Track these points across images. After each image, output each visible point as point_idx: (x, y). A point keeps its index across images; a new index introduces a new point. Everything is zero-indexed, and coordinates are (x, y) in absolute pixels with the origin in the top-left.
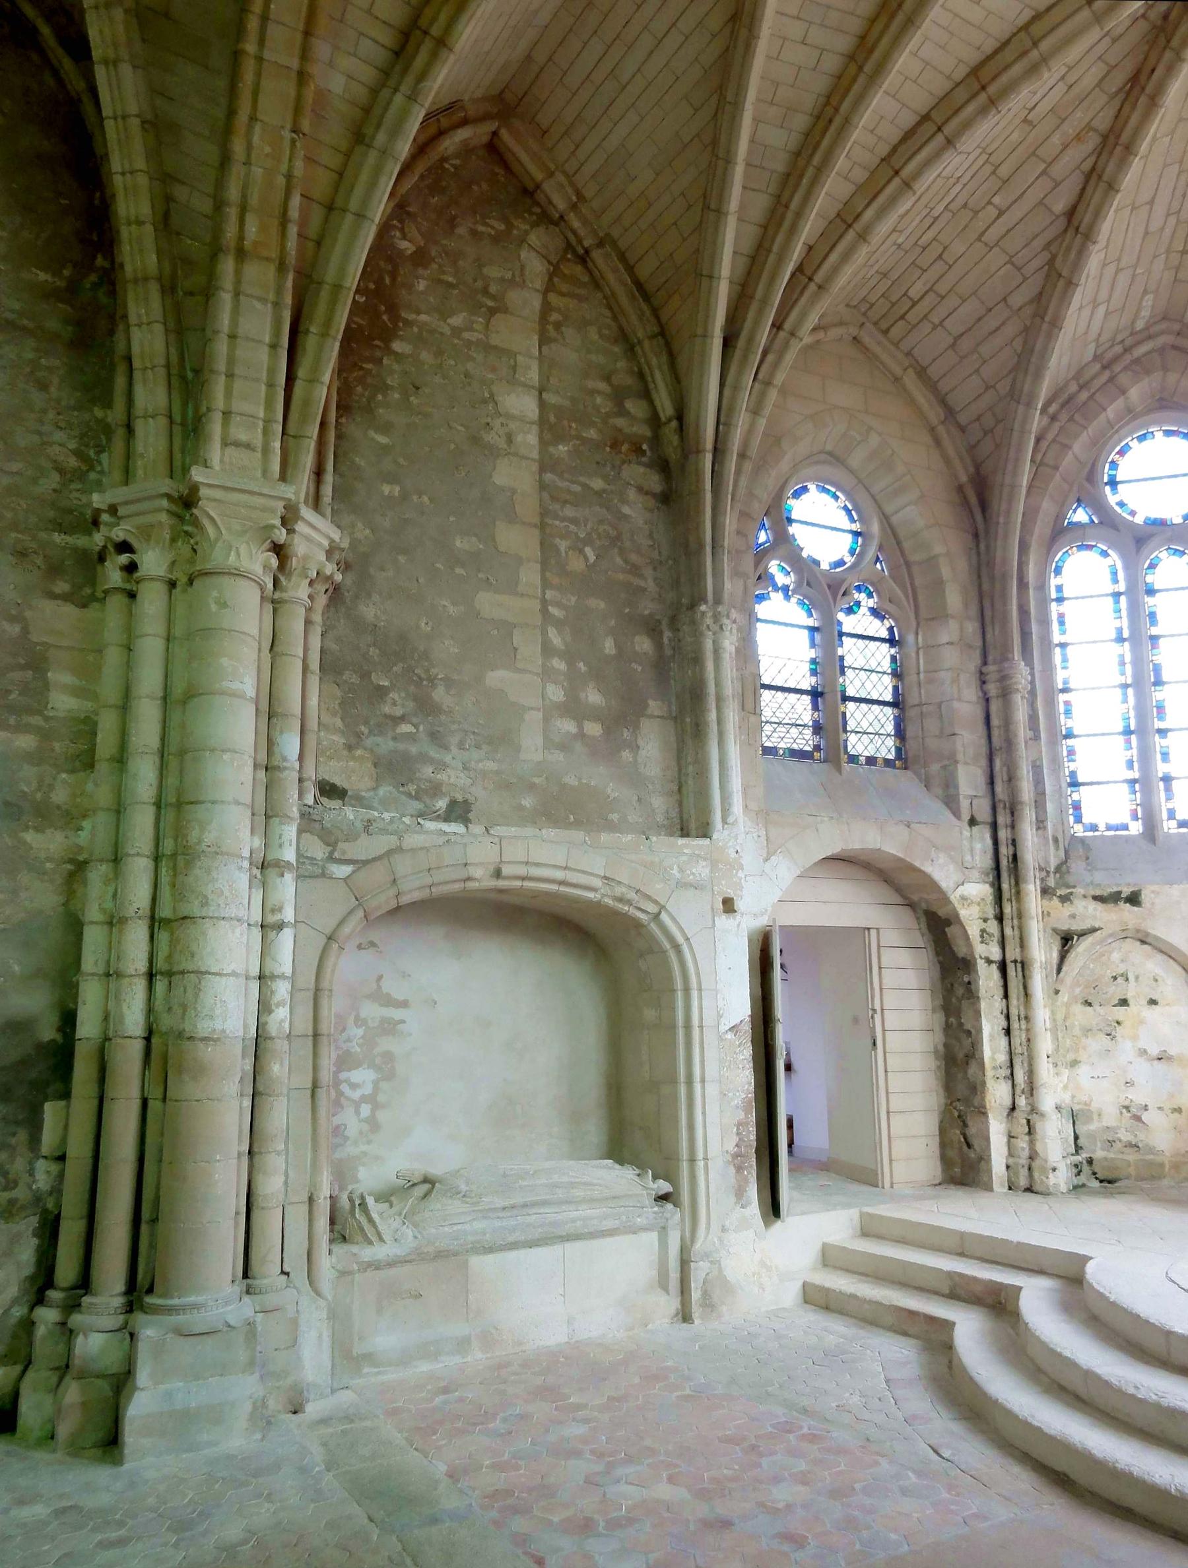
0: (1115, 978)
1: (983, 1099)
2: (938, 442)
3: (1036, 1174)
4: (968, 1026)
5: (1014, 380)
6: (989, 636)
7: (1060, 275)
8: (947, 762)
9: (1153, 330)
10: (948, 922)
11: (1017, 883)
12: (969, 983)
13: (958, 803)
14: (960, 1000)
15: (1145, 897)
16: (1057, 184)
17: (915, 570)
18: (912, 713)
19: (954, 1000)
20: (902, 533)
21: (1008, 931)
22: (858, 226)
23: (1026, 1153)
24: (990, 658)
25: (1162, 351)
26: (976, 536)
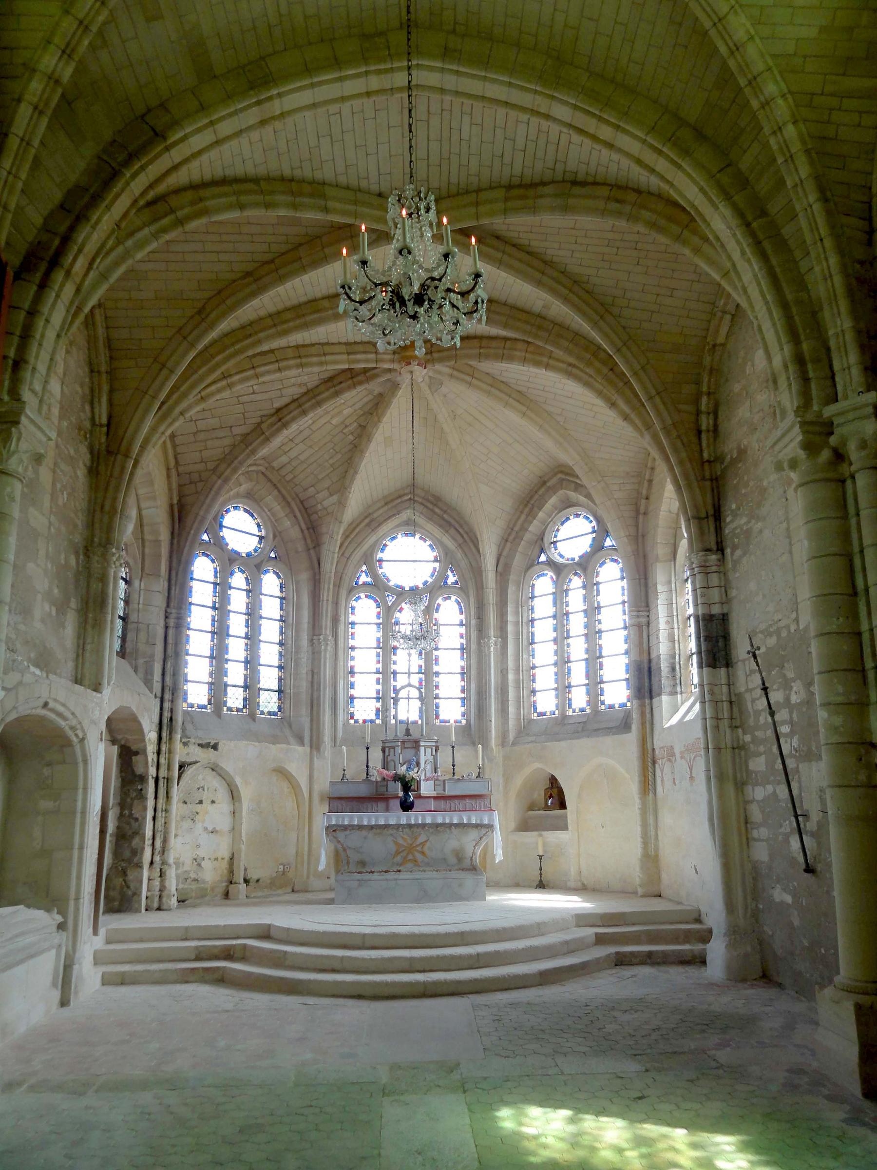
1: (141, 858)
2: (169, 476)
3: (164, 899)
4: (137, 815)
5: (219, 465)
6: (173, 592)
7: (263, 433)
10: (136, 753)
11: (170, 733)
13: (152, 684)
15: (220, 747)
16: (282, 396)
17: (147, 544)
18: (131, 626)
19: (129, 800)
20: (145, 521)
21: (162, 760)
22: (229, 380)
23: (158, 888)
24: (172, 605)
25: (257, 472)
26: (172, 533)
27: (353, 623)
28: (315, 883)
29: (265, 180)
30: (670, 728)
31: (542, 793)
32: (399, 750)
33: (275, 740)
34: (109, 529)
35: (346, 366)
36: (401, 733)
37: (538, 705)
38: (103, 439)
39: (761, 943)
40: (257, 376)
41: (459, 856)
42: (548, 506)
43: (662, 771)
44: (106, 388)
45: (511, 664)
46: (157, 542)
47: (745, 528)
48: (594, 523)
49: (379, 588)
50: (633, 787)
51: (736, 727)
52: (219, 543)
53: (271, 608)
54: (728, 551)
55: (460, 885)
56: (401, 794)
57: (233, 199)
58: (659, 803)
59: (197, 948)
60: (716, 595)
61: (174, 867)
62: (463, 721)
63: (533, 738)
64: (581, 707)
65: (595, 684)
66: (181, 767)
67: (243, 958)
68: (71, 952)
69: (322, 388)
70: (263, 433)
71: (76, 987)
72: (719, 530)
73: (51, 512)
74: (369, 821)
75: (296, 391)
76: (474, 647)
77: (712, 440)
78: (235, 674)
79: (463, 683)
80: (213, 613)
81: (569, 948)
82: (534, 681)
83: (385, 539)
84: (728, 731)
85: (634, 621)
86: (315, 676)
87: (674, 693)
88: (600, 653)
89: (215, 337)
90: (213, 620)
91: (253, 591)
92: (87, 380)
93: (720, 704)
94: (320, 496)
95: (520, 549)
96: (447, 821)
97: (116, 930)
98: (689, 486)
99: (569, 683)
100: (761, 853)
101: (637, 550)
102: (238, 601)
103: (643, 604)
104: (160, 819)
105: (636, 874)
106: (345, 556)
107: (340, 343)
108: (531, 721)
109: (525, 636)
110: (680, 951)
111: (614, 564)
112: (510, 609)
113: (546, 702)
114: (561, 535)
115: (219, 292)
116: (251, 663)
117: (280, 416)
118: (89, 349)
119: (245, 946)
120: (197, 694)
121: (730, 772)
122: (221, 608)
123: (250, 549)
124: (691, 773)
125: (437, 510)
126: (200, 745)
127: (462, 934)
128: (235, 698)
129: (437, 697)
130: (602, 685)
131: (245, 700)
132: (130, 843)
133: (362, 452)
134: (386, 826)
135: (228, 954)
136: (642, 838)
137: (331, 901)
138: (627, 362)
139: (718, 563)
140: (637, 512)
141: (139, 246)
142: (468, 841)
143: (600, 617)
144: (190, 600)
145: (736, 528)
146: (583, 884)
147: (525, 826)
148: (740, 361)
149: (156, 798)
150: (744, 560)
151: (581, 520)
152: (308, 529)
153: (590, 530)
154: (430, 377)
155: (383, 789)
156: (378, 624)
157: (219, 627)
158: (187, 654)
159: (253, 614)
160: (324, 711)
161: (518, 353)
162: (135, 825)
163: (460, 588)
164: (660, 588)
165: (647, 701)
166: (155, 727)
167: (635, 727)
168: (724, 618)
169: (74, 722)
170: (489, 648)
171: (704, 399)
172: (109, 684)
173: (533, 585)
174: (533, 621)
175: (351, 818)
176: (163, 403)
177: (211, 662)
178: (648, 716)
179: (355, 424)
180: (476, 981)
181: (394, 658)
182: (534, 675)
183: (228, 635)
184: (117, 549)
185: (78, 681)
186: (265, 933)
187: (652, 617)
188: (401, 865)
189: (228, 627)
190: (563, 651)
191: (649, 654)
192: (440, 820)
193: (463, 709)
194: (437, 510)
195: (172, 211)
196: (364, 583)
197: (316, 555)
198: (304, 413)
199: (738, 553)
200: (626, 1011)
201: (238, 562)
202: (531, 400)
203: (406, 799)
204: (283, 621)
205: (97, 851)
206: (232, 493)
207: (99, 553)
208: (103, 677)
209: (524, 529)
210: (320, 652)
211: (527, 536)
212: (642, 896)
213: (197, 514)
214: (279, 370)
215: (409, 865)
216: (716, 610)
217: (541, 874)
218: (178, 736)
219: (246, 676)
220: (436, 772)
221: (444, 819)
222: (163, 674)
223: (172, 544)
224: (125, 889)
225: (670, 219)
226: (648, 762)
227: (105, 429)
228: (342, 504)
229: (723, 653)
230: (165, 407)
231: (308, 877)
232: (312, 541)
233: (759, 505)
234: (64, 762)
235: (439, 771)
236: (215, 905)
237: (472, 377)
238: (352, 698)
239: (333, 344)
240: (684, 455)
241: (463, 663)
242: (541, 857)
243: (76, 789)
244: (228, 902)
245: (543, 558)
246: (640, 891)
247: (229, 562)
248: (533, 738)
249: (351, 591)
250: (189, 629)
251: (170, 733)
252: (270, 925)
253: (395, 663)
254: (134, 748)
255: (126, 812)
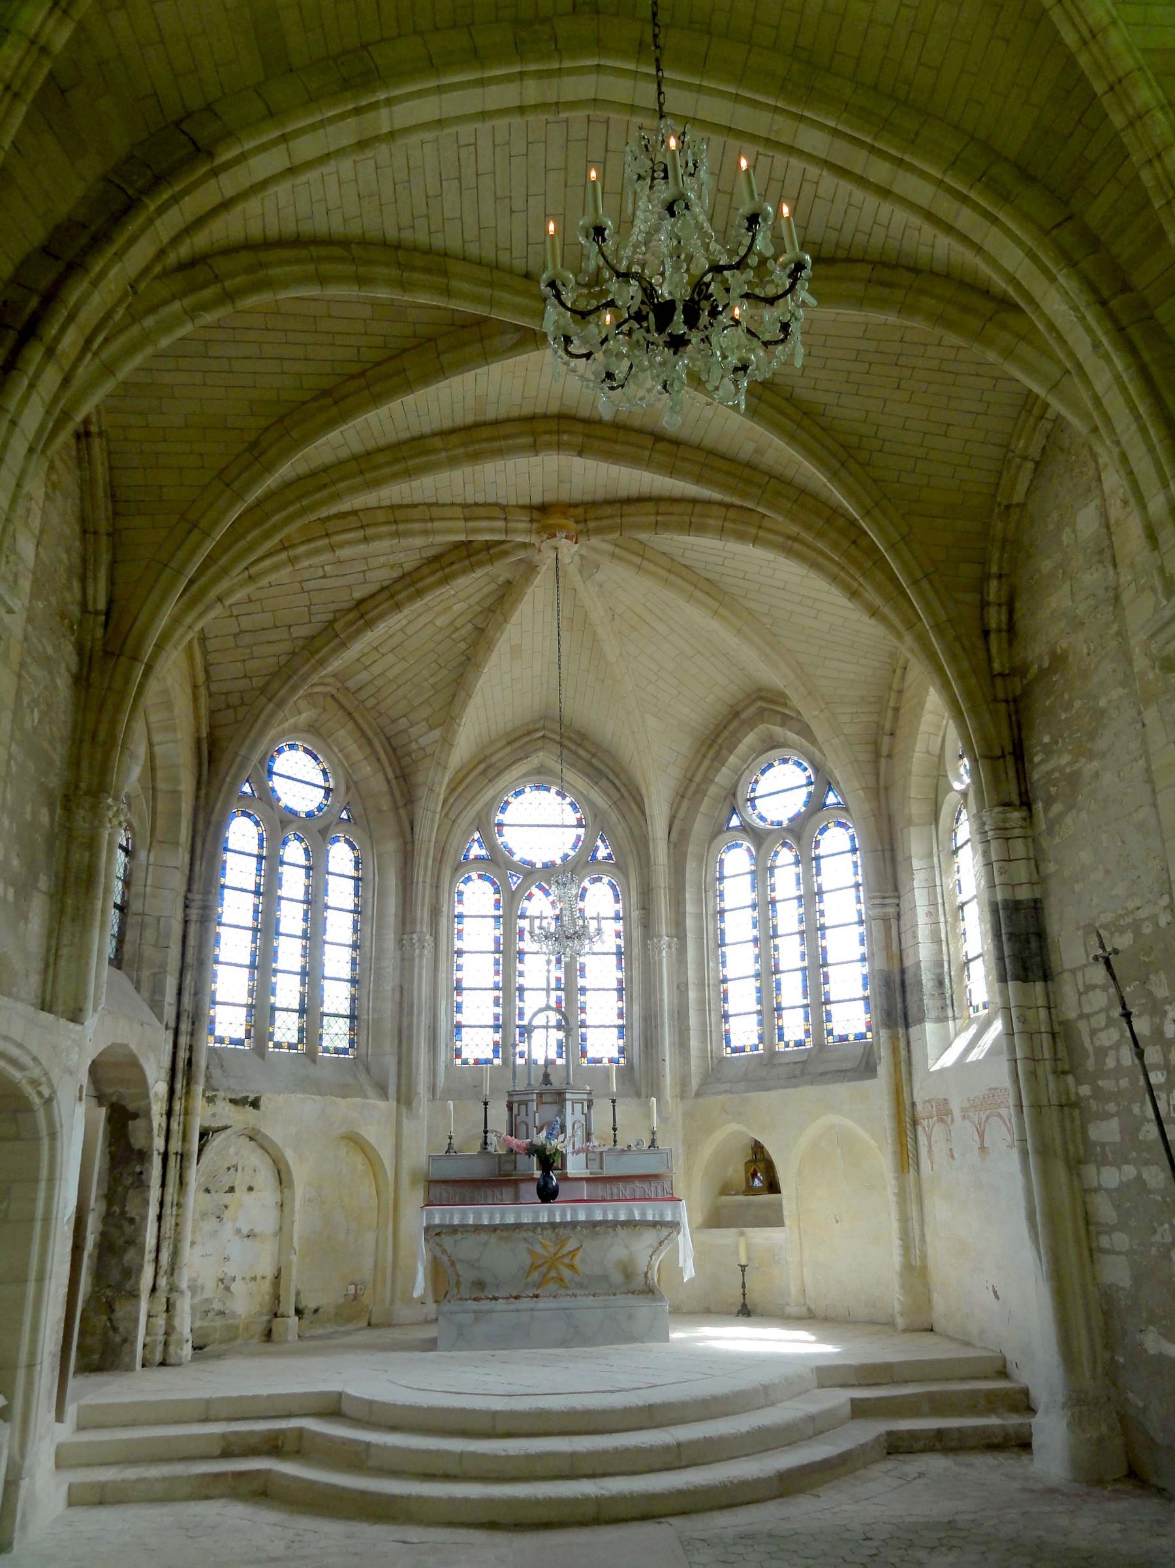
0: (229, 1169)
1: (137, 1282)
2: (196, 699)
3: (172, 1349)
6: (197, 868)
7: (337, 636)
8: (156, 970)
9: (327, 680)
10: (135, 1116)
11: (188, 1084)
12: (141, 1173)
13: (162, 1008)
14: (127, 1189)
16: (365, 582)
17: (160, 796)
18: (131, 920)
19: (120, 1189)
20: (158, 762)
21: (174, 1126)
22: (292, 553)
23: (162, 1331)
25: (325, 694)
26: (199, 782)
27: (460, 916)
28: (405, 1313)
29: (358, 244)
30: (942, 1071)
31: (741, 1168)
32: (533, 1106)
33: (345, 1091)
34: (104, 768)
35: (462, 537)
36: (536, 1080)
37: (732, 1037)
38: (99, 633)
39: (1122, 1418)
40: (332, 548)
41: (628, 1273)
42: (742, 748)
43: (929, 1138)
44: (105, 557)
45: (691, 975)
46: (175, 795)
47: (1068, 770)
48: (810, 772)
49: (498, 864)
50: (883, 1161)
51: (1064, 1073)
52: (268, 797)
53: (341, 893)
54: (1039, 806)
55: (630, 1317)
56: (537, 1174)
57: (311, 268)
58: (926, 1186)
59: (224, 1436)
60: (1022, 872)
61: (188, 1294)
62: (622, 1060)
63: (727, 1086)
64: (797, 1039)
65: (818, 1005)
66: (204, 1134)
67: (298, 1452)
68: (17, 1457)
69: (425, 570)
70: (337, 636)
71: (24, 1516)
72: (1022, 775)
73: (12, 738)
74: (491, 1218)
75: (384, 576)
76: (636, 951)
77: (1005, 645)
78: (287, 991)
79: (620, 1004)
80: (256, 901)
81: (813, 1428)
82: (725, 1000)
83: (506, 793)
84: (1051, 1078)
85: (877, 911)
86: (406, 995)
87: (942, 1019)
88: (825, 959)
89: (273, 486)
90: (256, 911)
91: (316, 869)
92: (77, 544)
93: (1036, 1037)
94: (414, 731)
95: (703, 808)
96: (610, 1217)
97: (93, 1408)
98: (974, 709)
99: (779, 1004)
100: (1117, 1273)
101: (879, 808)
102: (293, 882)
103: (890, 887)
104: (168, 1219)
105: (894, 1298)
106: (450, 820)
107: (453, 504)
108: (722, 1060)
109: (711, 935)
110: (984, 1429)
111: (842, 830)
113: (744, 1032)
114: (761, 790)
115: (281, 419)
116: (311, 975)
117: (363, 611)
118: (82, 499)
119: (301, 1431)
120: (229, 1023)
121: (1058, 1142)
122: (267, 892)
123: (312, 806)
124: (982, 1141)
125: (582, 752)
126: (233, 1101)
127: (650, 1408)
128: (286, 1028)
129: (583, 1025)
130: (828, 1007)
131: (301, 1030)
132: (121, 1258)
133: (479, 667)
134: (518, 1226)
135: (274, 1446)
136: (901, 1239)
137: (431, 1345)
138: (881, 531)
139: (1024, 824)
140: (877, 754)
141: (167, 327)
142: (641, 1247)
143: (822, 906)
144: (222, 881)
145: (1053, 771)
146: (809, 1309)
147: (716, 1219)
148: (1051, 527)
149: (163, 1185)
150: (1068, 820)
151: (790, 768)
152: (397, 778)
153: (804, 782)
154: (582, 557)
155: (508, 1167)
156: (497, 918)
157: (264, 922)
158: (217, 962)
159: (314, 902)
160: (419, 1047)
161: (710, 521)
162: (128, 1229)
163: (616, 865)
164: (916, 864)
165: (901, 1031)
166: (164, 1074)
167: (883, 1069)
168: (1036, 907)
169: (36, 1073)
170: (660, 952)
171: (994, 583)
172: (95, 1010)
173: (721, 861)
174: (722, 912)
175: (464, 1214)
176: (191, 582)
177: (252, 974)
178: (903, 1053)
179: (470, 626)
180: (680, 1493)
181: (520, 967)
182: (725, 992)
183: (278, 934)
184: (116, 799)
185: (45, 1006)
186: (334, 1408)
187: (905, 906)
188: (538, 1287)
189: (278, 921)
190: (769, 957)
191: (901, 960)
192: (599, 1217)
193: (621, 1042)
194: (582, 752)
195: (217, 279)
196: (476, 858)
197: (407, 819)
198: (398, 607)
199: (1057, 808)
200: (933, 1548)
201: (294, 825)
202: (725, 593)
203: (546, 1183)
204: (359, 913)
205: (67, 1282)
206: (286, 725)
207: (87, 806)
208: (86, 998)
209: (708, 780)
210: (413, 959)
211: (713, 790)
212: (904, 1331)
213: (236, 754)
214: (366, 540)
215: (552, 1287)
216: (1024, 894)
217: (744, 1295)
218: (199, 1088)
219: (302, 995)
220: (588, 1140)
221: (605, 1214)
222: (180, 993)
223: (197, 797)
224: (111, 1333)
225: (966, 309)
226: (906, 1123)
227: (103, 618)
228: (447, 742)
229: (1038, 959)
230: (195, 588)
231: (392, 1302)
232: (402, 795)
233: (1092, 736)
234: (17, 1137)
235: (593, 1138)
236: (253, 1355)
237: (642, 559)
238: (459, 1026)
239: (443, 505)
240: (965, 665)
241: (620, 975)
242: (743, 1268)
243: (36, 1180)
244: (270, 1347)
245: (735, 821)
246: (900, 1322)
247: (279, 824)
248: (727, 1086)
249: (457, 868)
250: (220, 924)
251: (188, 1084)
252: (340, 1394)
253: (521, 974)
254: (131, 1107)
255: (116, 1209)
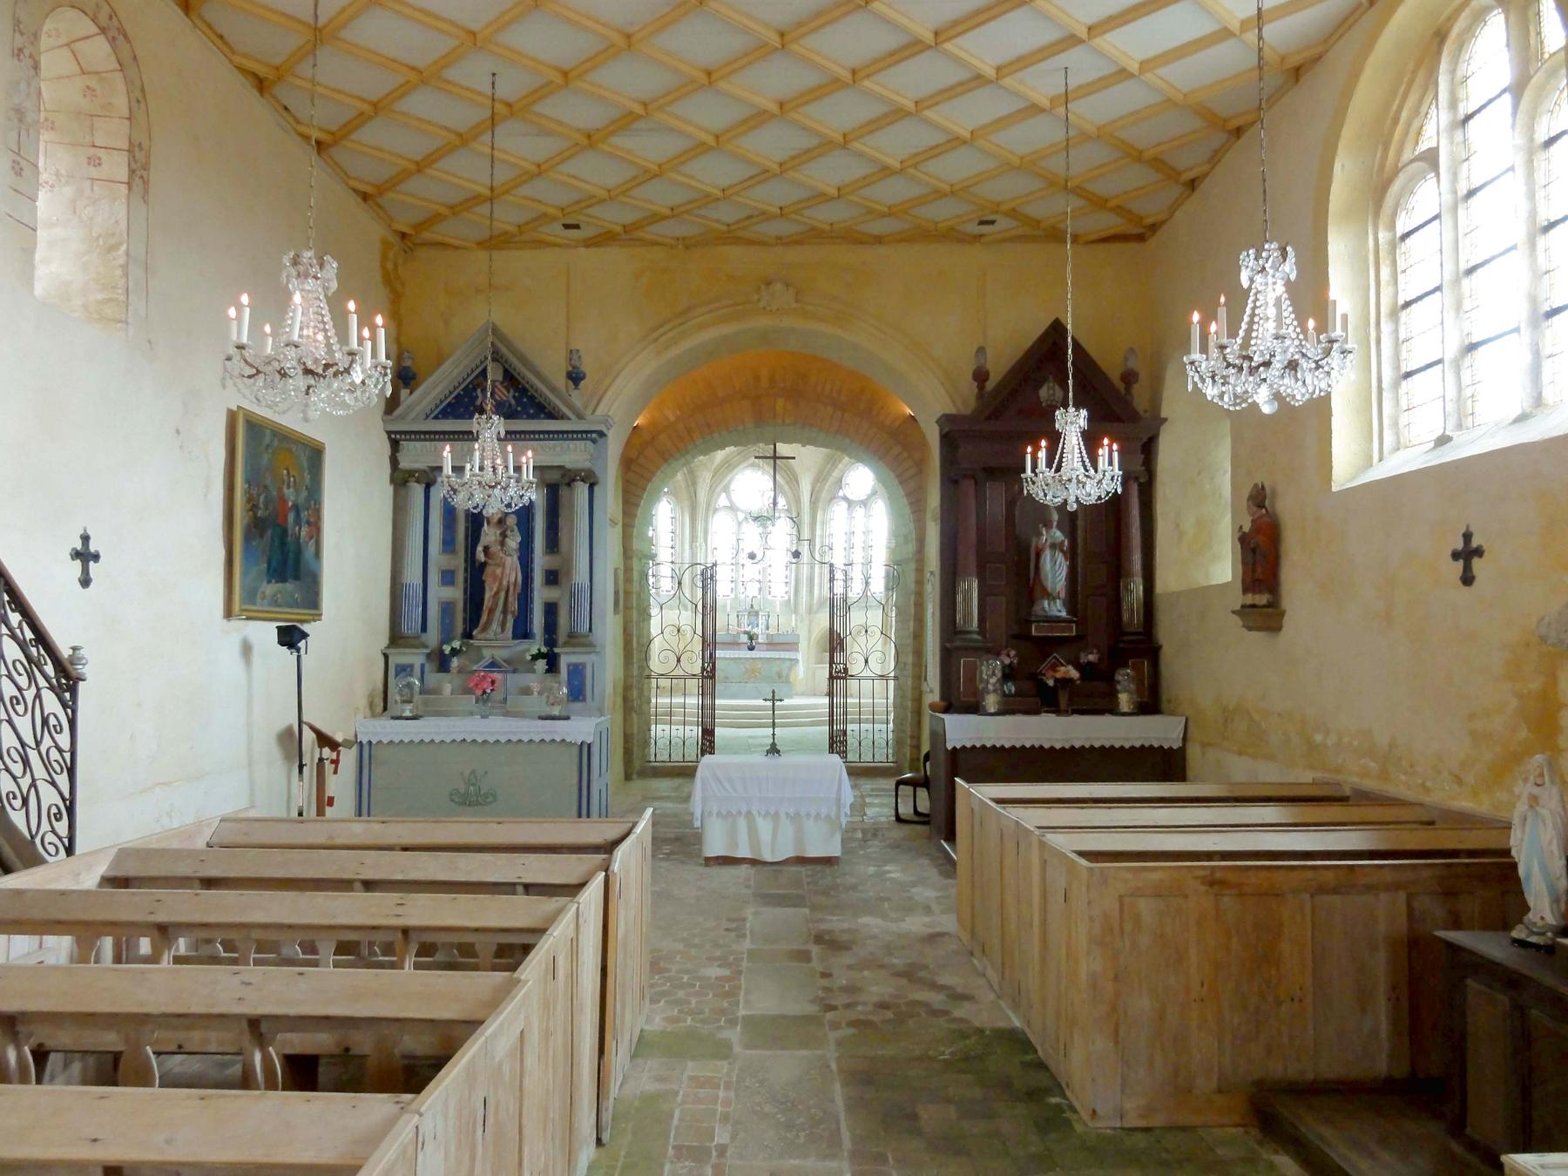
112: (818, 526)
209: (829, 474)
211: (831, 479)
245: (841, 493)
249: (716, 510)
